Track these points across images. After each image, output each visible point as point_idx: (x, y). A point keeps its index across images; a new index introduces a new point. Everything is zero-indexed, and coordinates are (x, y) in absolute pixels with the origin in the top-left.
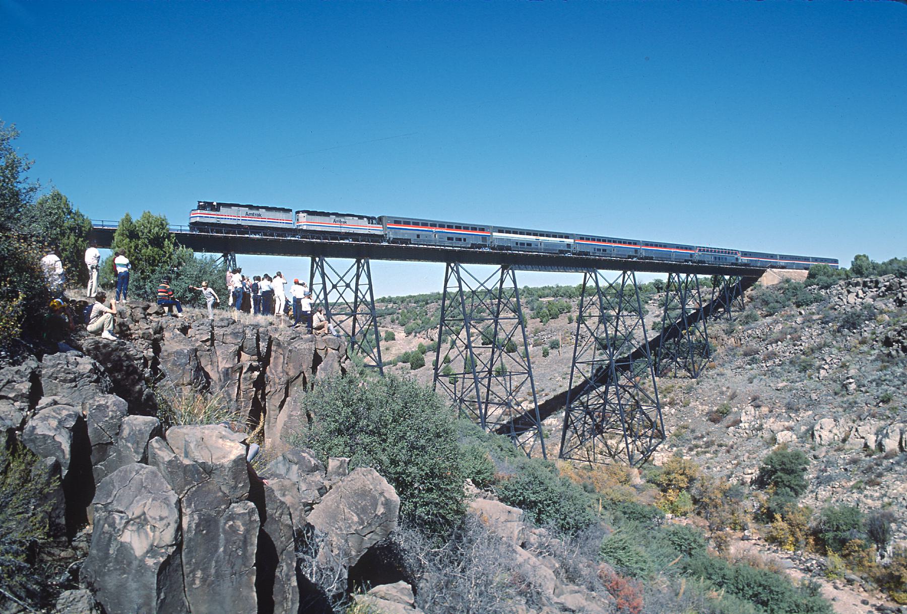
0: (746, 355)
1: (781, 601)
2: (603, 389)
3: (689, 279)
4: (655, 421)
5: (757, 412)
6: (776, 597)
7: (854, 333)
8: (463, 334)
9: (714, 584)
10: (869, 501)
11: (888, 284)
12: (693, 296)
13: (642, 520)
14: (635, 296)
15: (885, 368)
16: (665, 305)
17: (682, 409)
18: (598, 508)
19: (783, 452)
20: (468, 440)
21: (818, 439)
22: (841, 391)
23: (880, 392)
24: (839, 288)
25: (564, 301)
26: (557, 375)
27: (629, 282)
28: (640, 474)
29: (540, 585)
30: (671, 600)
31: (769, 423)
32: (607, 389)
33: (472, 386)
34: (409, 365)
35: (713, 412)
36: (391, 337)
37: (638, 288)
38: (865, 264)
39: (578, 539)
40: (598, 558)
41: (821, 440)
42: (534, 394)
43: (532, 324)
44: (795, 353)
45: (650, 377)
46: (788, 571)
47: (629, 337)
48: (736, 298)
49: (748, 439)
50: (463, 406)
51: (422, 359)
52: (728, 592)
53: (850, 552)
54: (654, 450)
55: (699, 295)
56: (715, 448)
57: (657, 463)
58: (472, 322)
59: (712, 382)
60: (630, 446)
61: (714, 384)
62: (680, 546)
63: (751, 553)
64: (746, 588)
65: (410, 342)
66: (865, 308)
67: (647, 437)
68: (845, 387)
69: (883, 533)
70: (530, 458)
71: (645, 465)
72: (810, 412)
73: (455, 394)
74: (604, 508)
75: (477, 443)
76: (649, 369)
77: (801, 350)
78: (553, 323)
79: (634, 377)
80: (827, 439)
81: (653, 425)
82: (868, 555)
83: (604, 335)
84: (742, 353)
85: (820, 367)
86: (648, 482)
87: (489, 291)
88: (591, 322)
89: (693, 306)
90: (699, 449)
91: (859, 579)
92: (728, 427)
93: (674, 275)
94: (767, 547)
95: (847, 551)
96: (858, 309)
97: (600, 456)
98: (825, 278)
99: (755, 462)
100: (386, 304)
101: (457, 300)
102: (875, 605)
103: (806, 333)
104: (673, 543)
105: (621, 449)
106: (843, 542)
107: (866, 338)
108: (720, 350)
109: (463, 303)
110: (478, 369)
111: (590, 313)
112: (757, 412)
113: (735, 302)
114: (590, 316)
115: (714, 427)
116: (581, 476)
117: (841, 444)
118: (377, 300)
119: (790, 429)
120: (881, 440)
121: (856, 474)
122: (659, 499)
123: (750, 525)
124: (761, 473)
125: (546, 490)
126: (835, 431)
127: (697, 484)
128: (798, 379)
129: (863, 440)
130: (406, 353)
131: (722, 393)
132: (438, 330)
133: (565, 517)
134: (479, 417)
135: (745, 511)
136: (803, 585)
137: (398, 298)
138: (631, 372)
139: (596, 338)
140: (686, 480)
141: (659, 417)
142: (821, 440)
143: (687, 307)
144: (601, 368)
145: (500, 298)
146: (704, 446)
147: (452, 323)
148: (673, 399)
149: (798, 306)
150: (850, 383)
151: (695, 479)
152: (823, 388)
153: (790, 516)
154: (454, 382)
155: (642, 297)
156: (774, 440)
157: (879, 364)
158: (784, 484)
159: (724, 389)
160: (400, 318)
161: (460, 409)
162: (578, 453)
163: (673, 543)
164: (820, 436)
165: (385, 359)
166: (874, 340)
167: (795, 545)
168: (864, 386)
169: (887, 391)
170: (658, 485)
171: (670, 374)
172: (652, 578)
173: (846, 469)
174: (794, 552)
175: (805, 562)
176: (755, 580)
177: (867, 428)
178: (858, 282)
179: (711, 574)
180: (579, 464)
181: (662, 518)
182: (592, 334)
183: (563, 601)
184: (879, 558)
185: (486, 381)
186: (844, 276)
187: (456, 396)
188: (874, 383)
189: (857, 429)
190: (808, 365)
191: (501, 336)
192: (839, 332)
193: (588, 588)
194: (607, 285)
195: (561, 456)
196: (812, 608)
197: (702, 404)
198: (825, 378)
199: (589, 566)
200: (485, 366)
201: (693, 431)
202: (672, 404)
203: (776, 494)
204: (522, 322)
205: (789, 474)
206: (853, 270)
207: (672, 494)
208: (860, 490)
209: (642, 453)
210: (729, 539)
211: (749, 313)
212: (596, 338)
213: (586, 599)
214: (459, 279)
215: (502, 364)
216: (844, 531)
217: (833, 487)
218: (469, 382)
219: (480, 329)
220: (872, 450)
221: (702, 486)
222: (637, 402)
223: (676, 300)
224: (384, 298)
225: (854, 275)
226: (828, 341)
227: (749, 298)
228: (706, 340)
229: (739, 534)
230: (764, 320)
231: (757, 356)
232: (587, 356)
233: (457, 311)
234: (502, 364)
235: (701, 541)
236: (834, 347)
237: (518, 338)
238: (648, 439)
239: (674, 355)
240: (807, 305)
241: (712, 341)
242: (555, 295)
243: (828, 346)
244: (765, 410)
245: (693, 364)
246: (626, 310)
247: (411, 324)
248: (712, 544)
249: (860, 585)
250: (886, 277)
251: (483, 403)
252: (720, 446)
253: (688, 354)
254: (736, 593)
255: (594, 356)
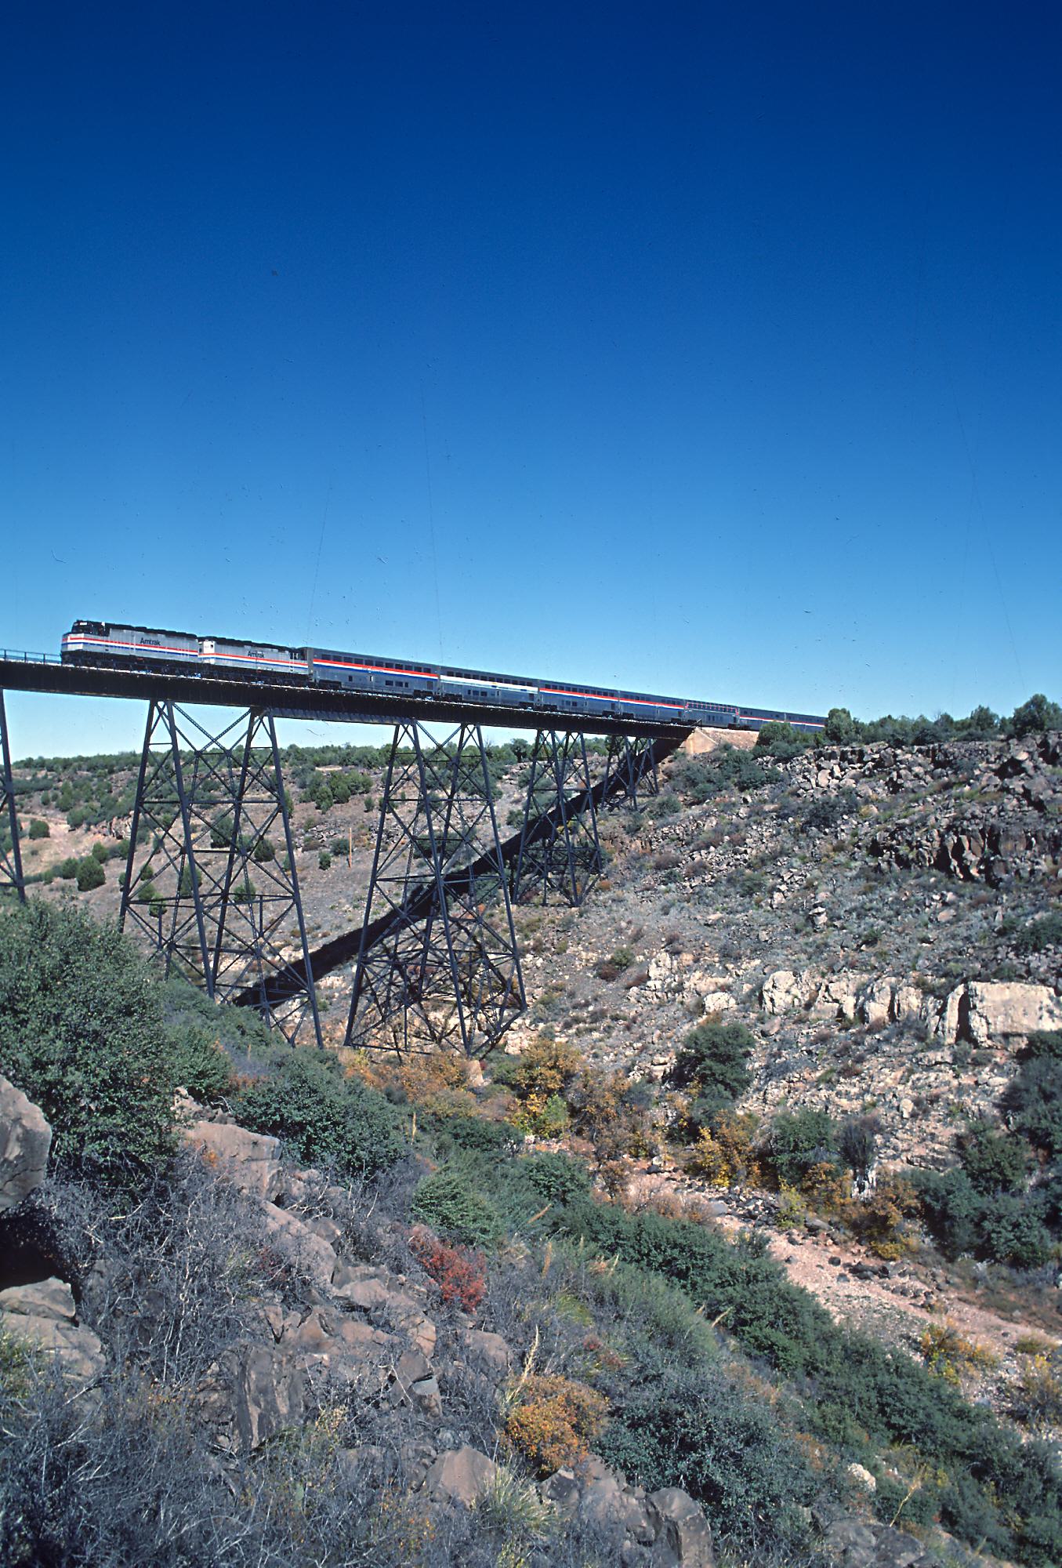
0: (658, 867)
1: (709, 1269)
2: (422, 924)
3: (571, 740)
4: (510, 979)
5: (675, 962)
6: (700, 1263)
7: (825, 834)
8: (178, 826)
9: (602, 1247)
10: (844, 1102)
11: (877, 756)
12: (576, 770)
13: (485, 1146)
14: (481, 767)
15: (871, 889)
16: (529, 783)
17: (555, 957)
18: (411, 1129)
19: (715, 1027)
20: (182, 1017)
21: (769, 1004)
22: (805, 926)
23: (862, 928)
24: (805, 762)
25: (359, 772)
26: (343, 901)
27: (471, 743)
28: (483, 1068)
29: (309, 1268)
30: (533, 1280)
31: (695, 980)
32: (429, 925)
33: (193, 920)
34: (74, 882)
35: (604, 962)
36: (41, 831)
37: (486, 754)
38: (844, 725)
39: (377, 1187)
40: (409, 1215)
41: (774, 1005)
42: (303, 933)
43: (302, 812)
44: (736, 866)
45: (503, 905)
46: (719, 1220)
47: (468, 836)
48: (644, 774)
49: (660, 1006)
50: (175, 956)
51: (101, 873)
52: (624, 1260)
53: (814, 1183)
54: (508, 1027)
55: (586, 767)
56: (607, 1022)
57: (512, 1050)
58: (194, 807)
59: (604, 913)
60: (467, 1022)
61: (607, 917)
62: (548, 1188)
63: (662, 1193)
64: (654, 1252)
65: (78, 841)
66: (843, 794)
67: (496, 1005)
68: (811, 920)
69: (864, 1151)
70: (294, 1047)
71: (492, 1054)
72: (757, 962)
73: (160, 934)
74: (422, 1128)
75: (199, 1021)
76: (502, 891)
77: (745, 861)
78: (339, 812)
79: (476, 905)
80: (783, 1004)
81: (505, 986)
82: (840, 1186)
83: (427, 832)
84: (653, 864)
85: (774, 889)
86: (496, 1082)
87: (226, 753)
88: (406, 809)
89: (575, 785)
90: (581, 1025)
91: (826, 1225)
92: (628, 988)
93: (546, 733)
94: (688, 1182)
95: (809, 1183)
96: (833, 796)
97: (415, 1040)
98: (785, 745)
99: (670, 1045)
100: (33, 771)
101: (168, 767)
102: (849, 1265)
103: (754, 833)
104: (537, 1184)
105: (452, 1027)
106: (803, 1169)
107: (843, 842)
108: (618, 860)
109: (178, 772)
110: (204, 889)
111: (403, 795)
112: (675, 962)
113: (643, 781)
114: (404, 800)
115: (606, 989)
116: (381, 1075)
117: (803, 1012)
118: (16, 763)
119: (725, 988)
120: (863, 1004)
121: (825, 1060)
122: (515, 1111)
123: (661, 1147)
124: (679, 1061)
125: (321, 1102)
126: (795, 991)
127: (577, 1084)
128: (740, 908)
129: (836, 1005)
130: (69, 862)
131: (620, 931)
132: (131, 820)
133: (354, 1148)
134: (203, 976)
135: (654, 1126)
136: (743, 1240)
137: (56, 760)
138: (471, 896)
139: (413, 838)
140: (558, 1077)
141: (516, 972)
142: (774, 1005)
143: (566, 787)
144: (420, 888)
145: (246, 765)
146: (588, 1020)
147: (157, 807)
148: (538, 941)
149: (742, 790)
150: (819, 914)
151: (574, 1075)
152: (777, 922)
153: (725, 1130)
154: (159, 912)
155: (492, 769)
156: (701, 1007)
157: (862, 883)
158: (716, 1080)
159: (623, 924)
160: (61, 797)
161: (168, 961)
162: (377, 1036)
163: (537, 1184)
164: (772, 1000)
165: (27, 872)
166: (856, 845)
167: (730, 1177)
168: (839, 918)
169: (872, 926)
170: (513, 1087)
171: (536, 900)
172: (501, 1246)
173: (809, 1052)
174: (729, 1188)
175: (745, 1204)
176: (668, 1239)
177: (843, 984)
178: (833, 752)
179: (597, 1233)
180: (380, 1054)
181: (520, 1142)
182: (406, 831)
183: (349, 1293)
184: (857, 1190)
185: (216, 912)
186: (812, 742)
187: (161, 938)
188: (854, 914)
189: (827, 987)
190: (755, 885)
191: (247, 832)
192: (802, 831)
193: (392, 1269)
194: (433, 746)
195: (349, 1041)
196: (755, 1276)
197: (586, 949)
198: (781, 906)
199: (393, 1231)
200: (217, 884)
201: (572, 995)
202: (538, 950)
203: (703, 1095)
204: (284, 808)
205: (723, 1063)
206: (827, 734)
207: (535, 1103)
208: (831, 1084)
209: (487, 1033)
210: (627, 1173)
211: (666, 798)
212: (413, 838)
213: (388, 1288)
214: (173, 730)
215: (247, 880)
216: (806, 1151)
217: (789, 1082)
218: (185, 914)
219: (207, 819)
220: (849, 1020)
221: (585, 1086)
222: (480, 947)
223: (548, 776)
224: (30, 760)
225: (827, 742)
226: (787, 846)
227: (666, 774)
228: (596, 843)
229: (644, 1164)
230: (689, 812)
231: (677, 870)
232: (397, 869)
233: (166, 786)
234: (247, 880)
235: (583, 1178)
236: (796, 855)
237: (276, 835)
238: (497, 1010)
239: (542, 868)
240: (756, 788)
241: (606, 846)
242: (343, 762)
243: (787, 855)
244: (687, 958)
245: (574, 882)
246: (465, 790)
247: (81, 808)
248: (600, 1181)
249: (828, 1235)
250: (874, 746)
251: (211, 950)
252: (616, 1018)
253: (565, 865)
254: (638, 1261)
255: (408, 868)
